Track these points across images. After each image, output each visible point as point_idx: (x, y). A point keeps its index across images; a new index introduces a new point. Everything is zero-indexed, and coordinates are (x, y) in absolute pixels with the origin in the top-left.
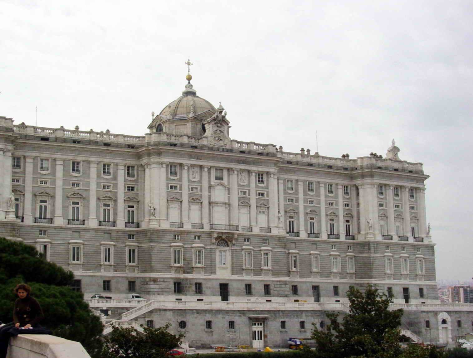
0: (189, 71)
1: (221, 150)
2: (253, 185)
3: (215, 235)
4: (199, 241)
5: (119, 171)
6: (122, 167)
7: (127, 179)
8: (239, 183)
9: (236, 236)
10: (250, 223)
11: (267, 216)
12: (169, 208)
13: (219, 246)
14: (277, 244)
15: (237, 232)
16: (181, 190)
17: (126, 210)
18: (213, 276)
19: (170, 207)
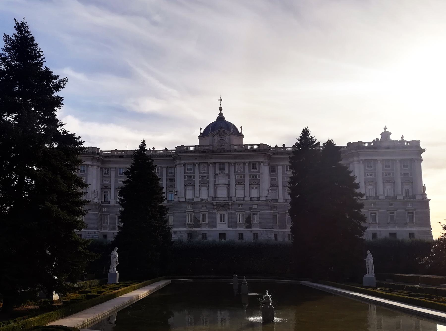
0: (221, 105)
1: (223, 151)
2: (247, 171)
3: (215, 204)
4: (205, 208)
5: (163, 171)
6: (165, 169)
7: (168, 175)
8: (236, 171)
9: (230, 204)
10: (245, 195)
11: (258, 190)
12: (187, 190)
13: (220, 210)
14: (265, 207)
15: (231, 201)
16: (194, 178)
17: (167, 193)
18: (214, 229)
19: (188, 189)
